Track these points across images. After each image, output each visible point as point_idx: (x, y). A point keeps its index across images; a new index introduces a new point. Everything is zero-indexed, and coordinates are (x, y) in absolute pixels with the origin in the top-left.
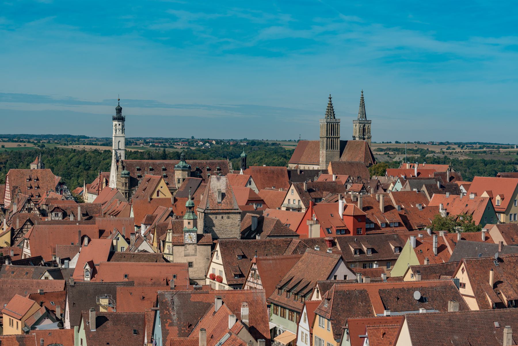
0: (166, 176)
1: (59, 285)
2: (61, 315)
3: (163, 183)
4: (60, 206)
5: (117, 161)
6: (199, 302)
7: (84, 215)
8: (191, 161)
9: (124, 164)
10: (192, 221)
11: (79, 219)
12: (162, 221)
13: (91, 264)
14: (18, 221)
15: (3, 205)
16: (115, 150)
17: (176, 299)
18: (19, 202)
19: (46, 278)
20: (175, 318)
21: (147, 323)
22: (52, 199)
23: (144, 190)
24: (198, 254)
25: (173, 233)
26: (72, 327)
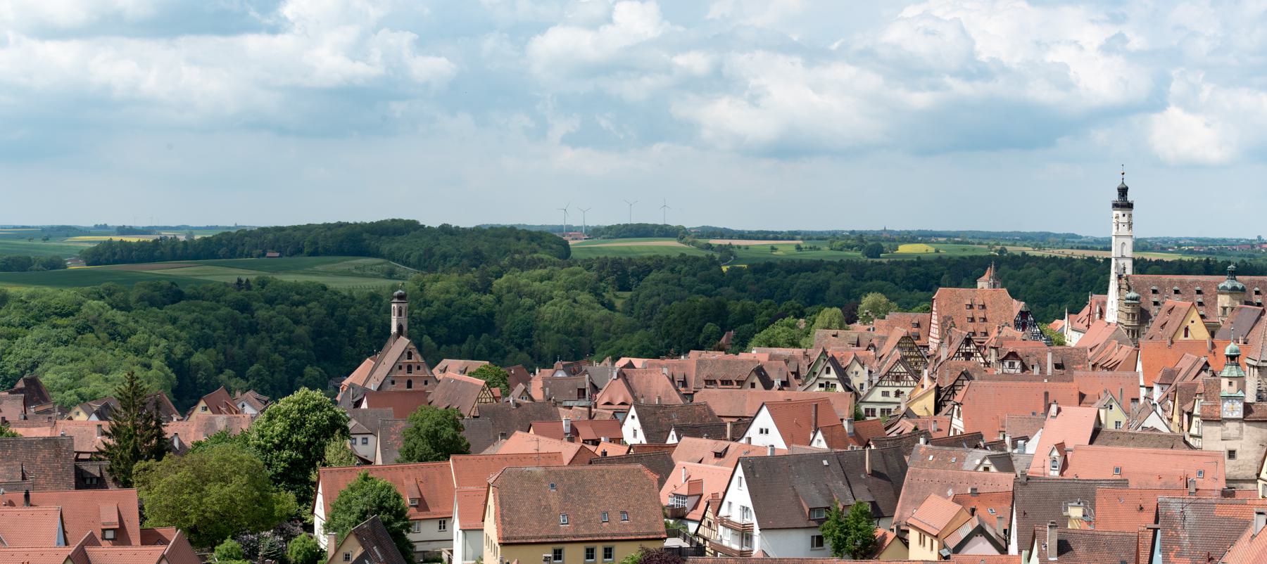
0: (1200, 304)
1: (1005, 481)
2: (1005, 531)
3: (1195, 315)
4: (1019, 351)
5: (1120, 277)
6: (1229, 519)
7: (1058, 366)
8: (1246, 278)
9: (1131, 282)
10: (1235, 383)
11: (1049, 370)
12: (1189, 379)
13: (1060, 447)
14: (947, 374)
15: (927, 347)
16: (1117, 259)
17: (1188, 511)
18: (950, 343)
19: (986, 469)
20: (1186, 542)
21: (1141, 551)
22: (1007, 338)
23: (1162, 327)
24: (1245, 436)
25: (1206, 399)
26: (1020, 552)
